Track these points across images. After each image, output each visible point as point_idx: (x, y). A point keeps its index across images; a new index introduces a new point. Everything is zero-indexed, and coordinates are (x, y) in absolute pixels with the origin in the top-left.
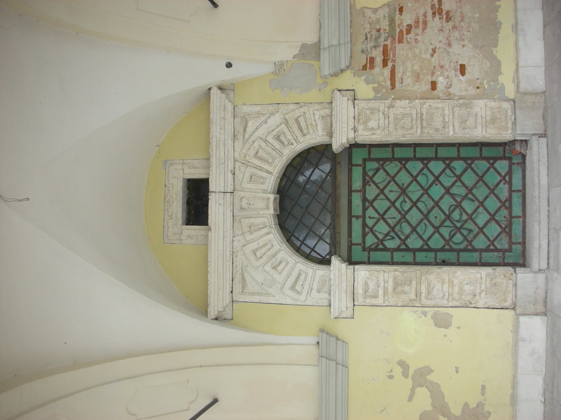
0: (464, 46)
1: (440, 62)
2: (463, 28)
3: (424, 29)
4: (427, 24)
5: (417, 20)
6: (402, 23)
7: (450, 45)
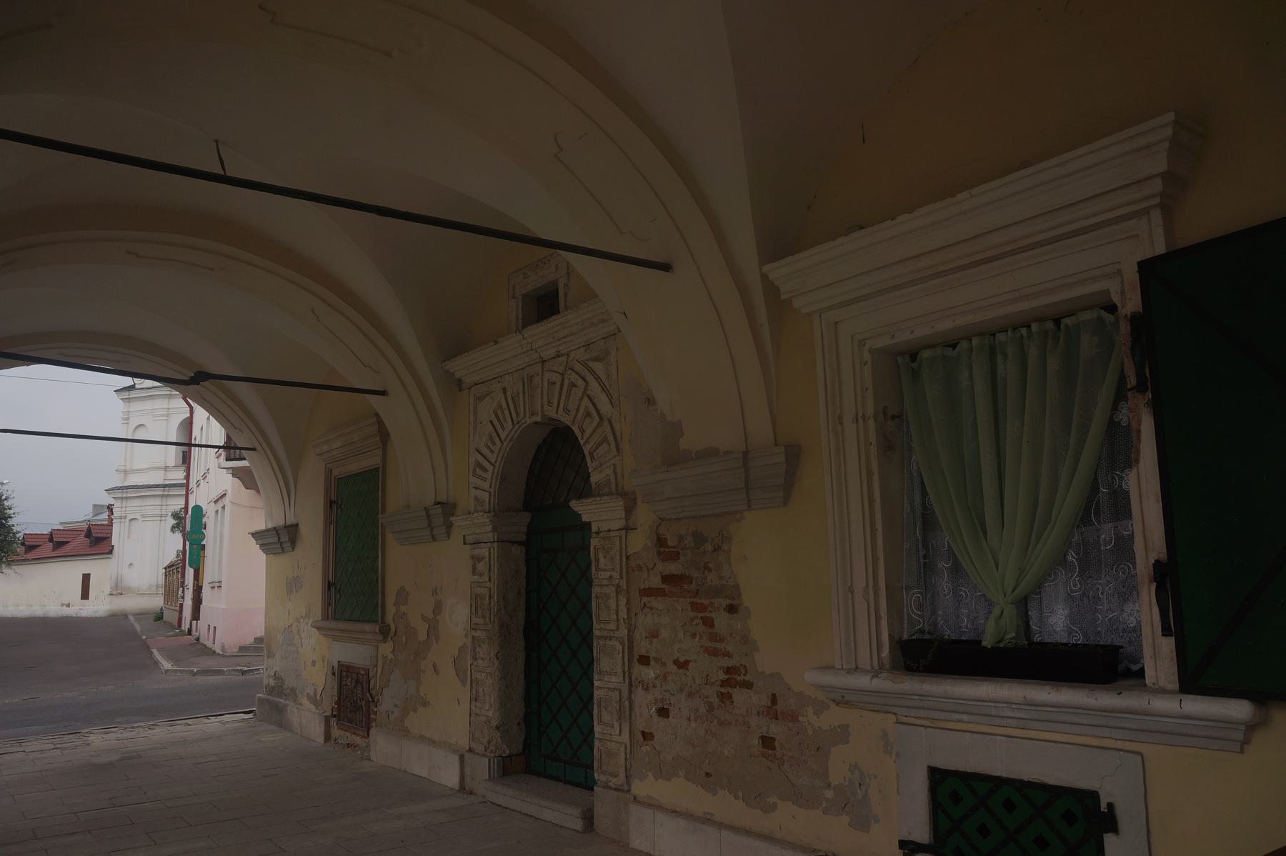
0: (689, 719)
1: (671, 675)
3: (706, 650)
7: (690, 695)
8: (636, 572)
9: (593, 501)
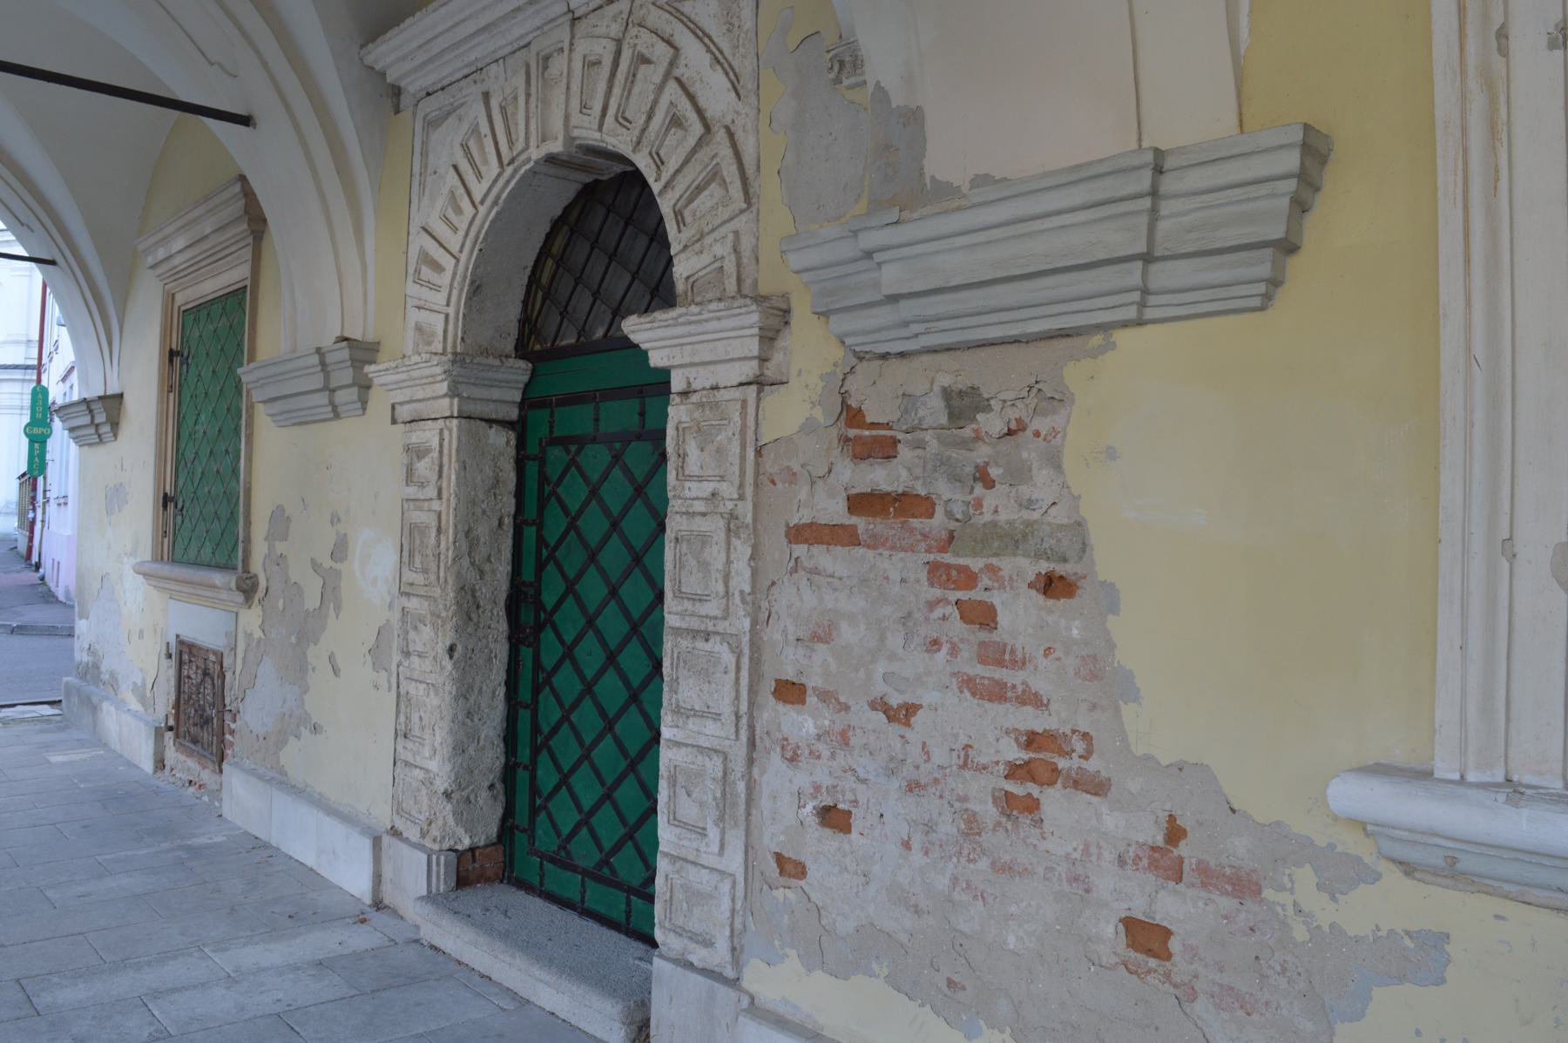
0: (907, 845)
1: (858, 731)
2: (969, 861)
3: (970, 685)
4: (990, 700)
5: (1007, 657)
6: (1002, 587)
7: (913, 787)
8: (780, 485)
9: (681, 316)
